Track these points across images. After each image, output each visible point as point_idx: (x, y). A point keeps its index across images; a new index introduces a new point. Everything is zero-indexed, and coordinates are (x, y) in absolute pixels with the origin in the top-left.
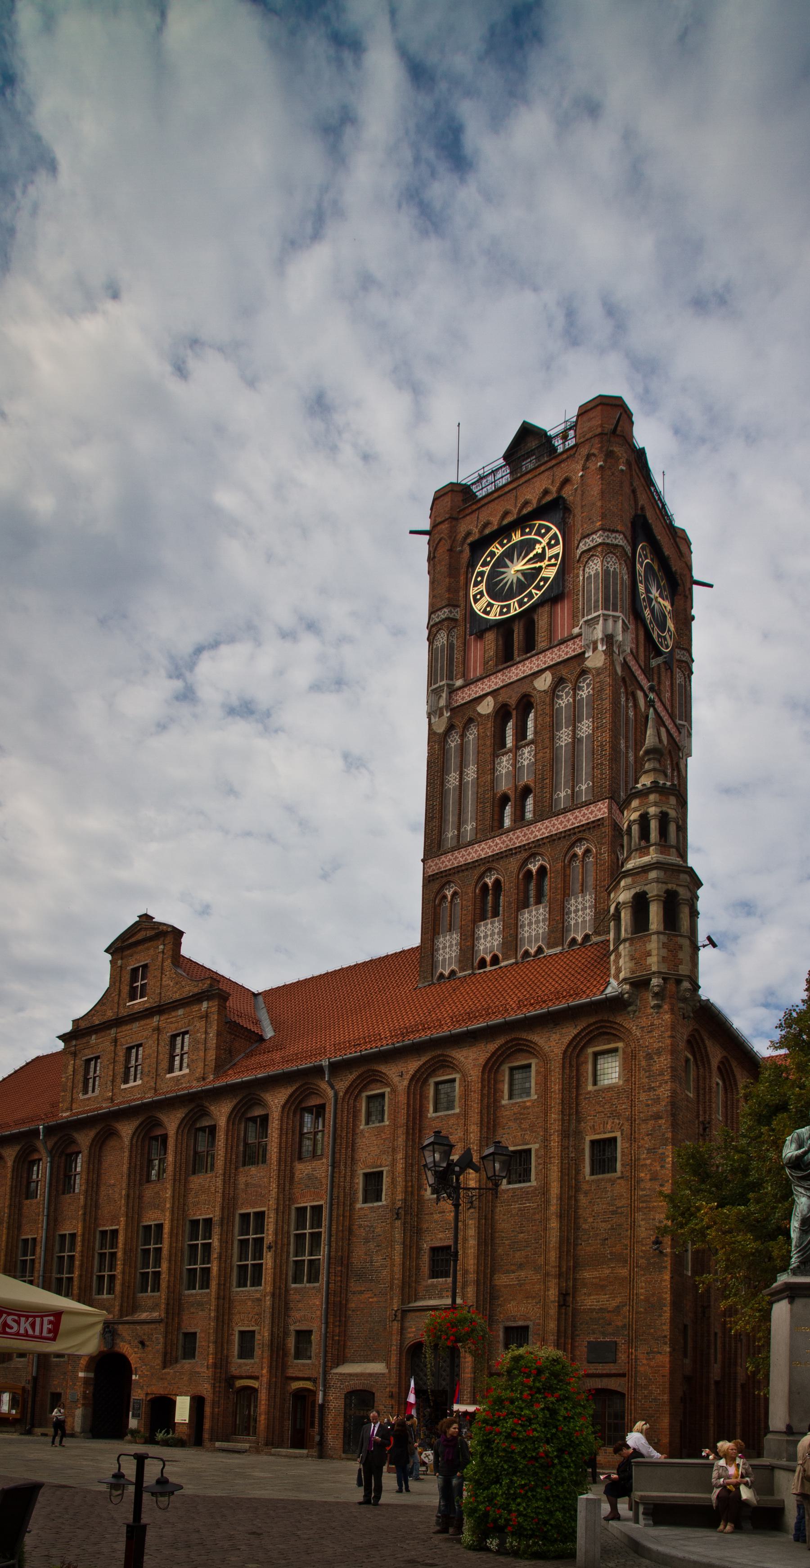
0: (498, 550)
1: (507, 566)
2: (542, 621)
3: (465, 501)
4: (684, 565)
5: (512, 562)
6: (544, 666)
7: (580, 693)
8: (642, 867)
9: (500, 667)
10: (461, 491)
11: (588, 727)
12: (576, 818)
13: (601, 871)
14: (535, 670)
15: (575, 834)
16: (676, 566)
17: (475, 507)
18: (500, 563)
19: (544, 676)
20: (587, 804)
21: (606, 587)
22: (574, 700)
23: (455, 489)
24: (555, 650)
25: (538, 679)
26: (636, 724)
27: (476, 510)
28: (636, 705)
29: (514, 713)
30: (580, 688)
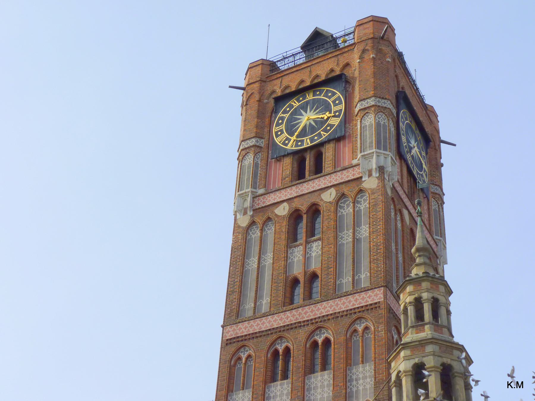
0: (295, 103)
1: (302, 115)
2: (328, 152)
3: (272, 71)
4: (434, 129)
5: (306, 112)
6: (330, 185)
7: (359, 206)
8: (419, 341)
9: (294, 183)
10: (270, 65)
11: (365, 231)
12: (356, 300)
13: (379, 346)
14: (321, 188)
15: (355, 313)
16: (428, 129)
17: (279, 75)
18: (296, 112)
19: (329, 191)
20: (366, 290)
21: (378, 134)
22: (354, 211)
23: (265, 63)
24: (339, 174)
25: (325, 193)
26: (403, 233)
27: (279, 77)
28: (402, 220)
29: (305, 216)
30: (358, 202)
